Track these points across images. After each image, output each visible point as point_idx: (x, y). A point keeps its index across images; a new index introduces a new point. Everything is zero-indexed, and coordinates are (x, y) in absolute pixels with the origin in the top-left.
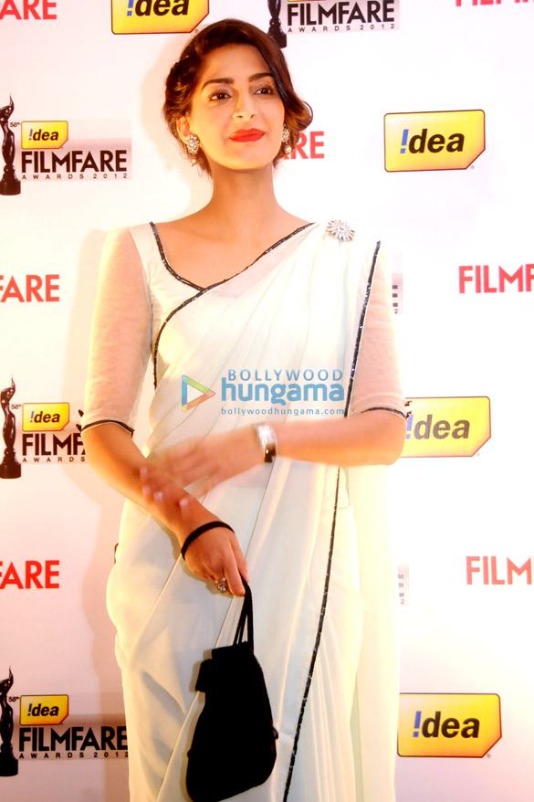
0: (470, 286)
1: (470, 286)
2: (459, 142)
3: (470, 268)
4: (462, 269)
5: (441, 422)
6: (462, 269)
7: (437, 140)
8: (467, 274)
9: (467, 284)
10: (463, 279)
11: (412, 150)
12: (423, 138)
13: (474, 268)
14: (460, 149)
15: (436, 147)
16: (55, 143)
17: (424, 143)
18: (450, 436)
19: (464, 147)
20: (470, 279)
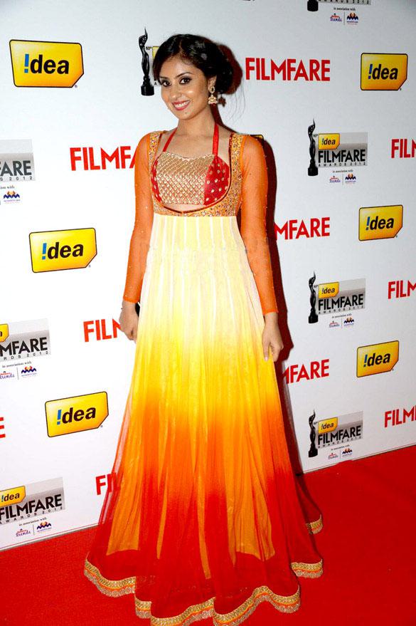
0: (93, 336)
1: (93, 336)
2: (80, 249)
3: (92, 322)
4: (86, 324)
5: (77, 412)
6: (86, 324)
7: (66, 249)
8: (90, 327)
9: (90, 334)
10: (87, 331)
11: (50, 257)
12: (57, 248)
13: (95, 322)
14: (81, 254)
15: (65, 254)
17: (56, 252)
18: (84, 418)
19: (84, 253)
20: (92, 330)
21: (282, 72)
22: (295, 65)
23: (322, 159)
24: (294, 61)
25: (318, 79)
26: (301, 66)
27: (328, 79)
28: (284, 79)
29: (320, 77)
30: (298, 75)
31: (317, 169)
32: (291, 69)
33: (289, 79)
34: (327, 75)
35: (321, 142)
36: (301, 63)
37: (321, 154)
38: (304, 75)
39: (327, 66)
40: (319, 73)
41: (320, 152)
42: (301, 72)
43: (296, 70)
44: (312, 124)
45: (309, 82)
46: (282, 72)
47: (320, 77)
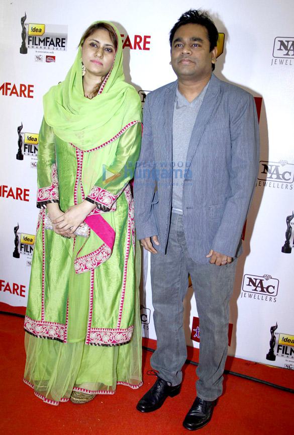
16: (40, 34)
21: (2, 89)
22: (11, 87)
23: (27, 150)
24: (10, 84)
25: (25, 96)
26: (14, 87)
27: (32, 97)
28: (3, 94)
29: (27, 95)
30: (12, 93)
31: (23, 156)
32: (7, 89)
33: (6, 94)
34: (31, 94)
35: (26, 138)
36: (14, 85)
37: (26, 146)
38: (16, 93)
39: (31, 89)
40: (26, 93)
41: (25, 145)
42: (14, 91)
43: (11, 89)
44: (21, 125)
45: (19, 97)
46: (2, 89)
47: (27, 95)
